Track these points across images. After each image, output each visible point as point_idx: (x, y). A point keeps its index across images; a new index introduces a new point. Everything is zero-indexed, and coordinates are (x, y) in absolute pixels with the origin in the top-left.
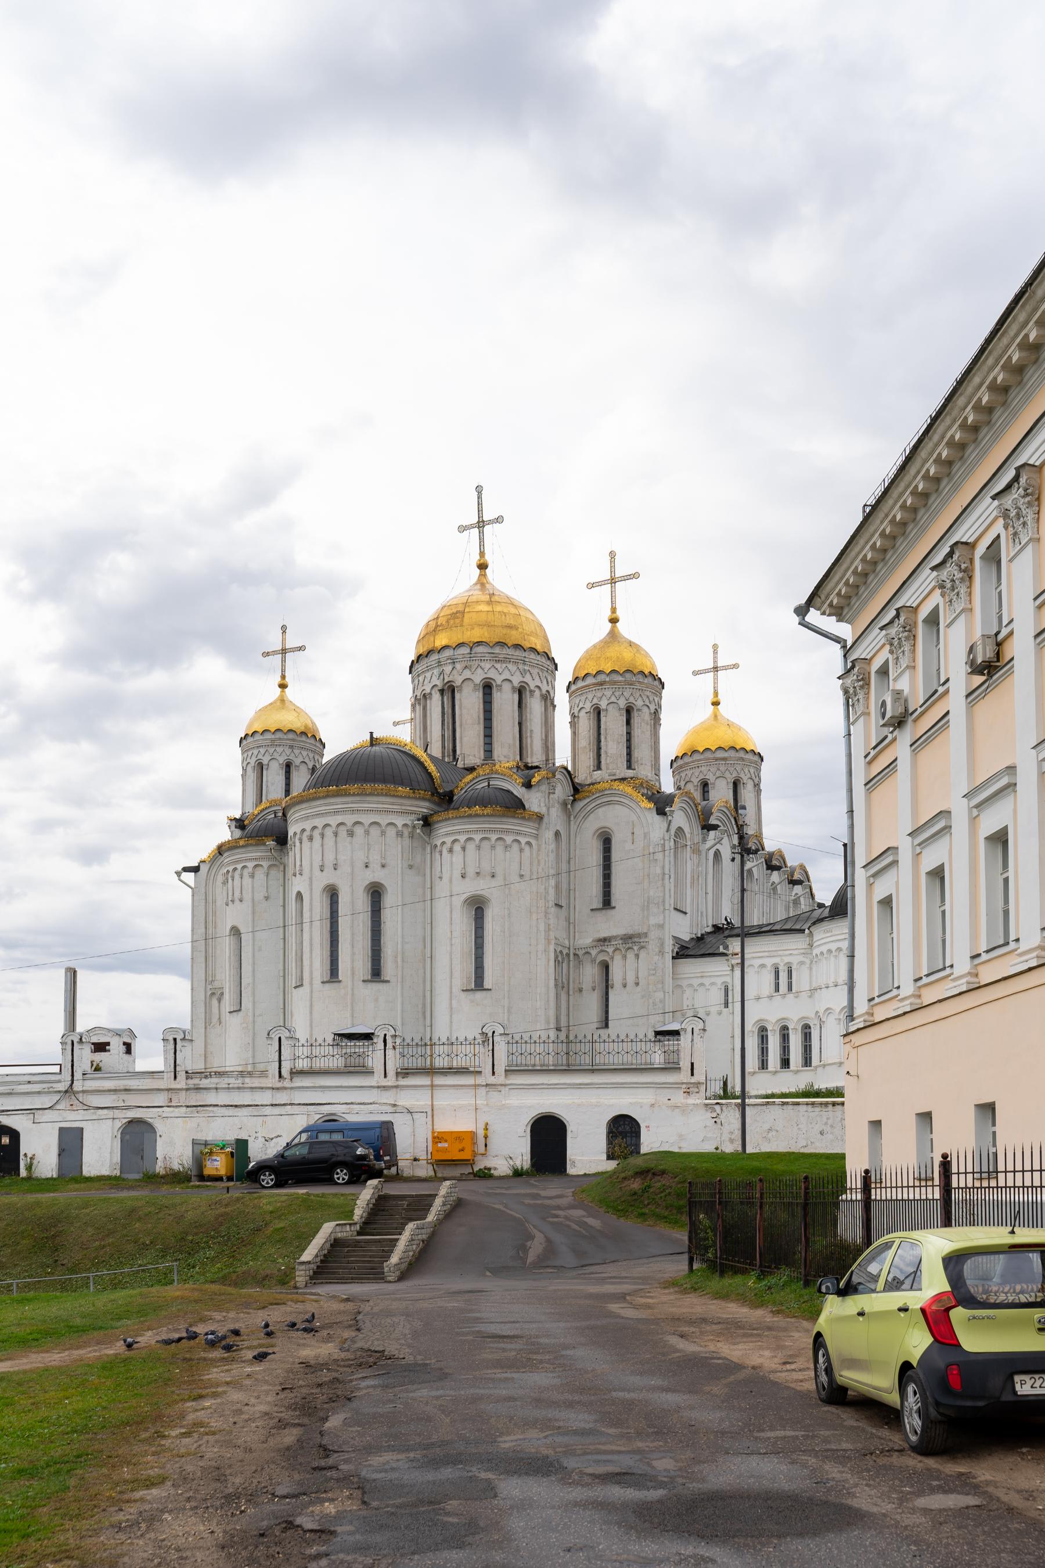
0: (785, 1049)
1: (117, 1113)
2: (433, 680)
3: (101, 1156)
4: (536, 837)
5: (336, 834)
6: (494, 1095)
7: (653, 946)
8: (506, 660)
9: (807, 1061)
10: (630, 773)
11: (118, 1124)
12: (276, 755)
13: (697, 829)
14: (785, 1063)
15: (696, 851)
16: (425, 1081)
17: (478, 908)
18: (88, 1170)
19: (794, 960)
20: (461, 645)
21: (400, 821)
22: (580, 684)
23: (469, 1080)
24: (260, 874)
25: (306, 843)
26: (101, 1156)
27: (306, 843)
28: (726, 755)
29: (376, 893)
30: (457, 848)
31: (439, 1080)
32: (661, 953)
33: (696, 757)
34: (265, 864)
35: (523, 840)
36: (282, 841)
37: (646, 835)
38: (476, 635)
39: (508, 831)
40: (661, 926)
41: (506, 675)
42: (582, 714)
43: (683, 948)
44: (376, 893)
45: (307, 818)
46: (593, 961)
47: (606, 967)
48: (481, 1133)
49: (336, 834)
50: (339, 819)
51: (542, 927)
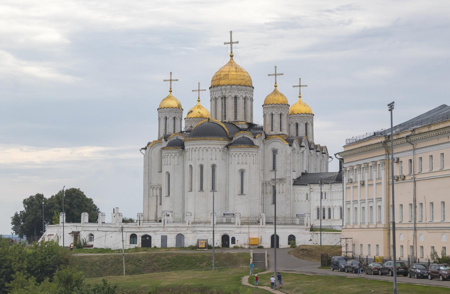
0: (324, 214)
1: (175, 232)
2: (218, 94)
3: (171, 243)
4: (257, 152)
5: (203, 150)
6: (263, 230)
7: (288, 183)
8: (241, 90)
9: (330, 217)
10: (281, 133)
11: (176, 235)
12: (171, 115)
13: (298, 146)
14: (324, 218)
15: (298, 153)
16: (247, 226)
17: (242, 172)
18: (168, 246)
19: (327, 191)
20: (228, 85)
21: (220, 147)
22: (267, 106)
23: (257, 226)
24: (176, 157)
25: (193, 152)
26: (171, 243)
27: (193, 152)
28: (304, 115)
29: (214, 167)
30: (236, 155)
31: (250, 226)
32: (290, 184)
33: (294, 115)
34: (178, 154)
35: (254, 154)
36: (183, 148)
37: (286, 151)
38: (233, 82)
39: (250, 152)
40: (290, 177)
41: (241, 94)
42: (267, 114)
43: (295, 182)
44: (214, 167)
45: (194, 145)
46: (270, 185)
47: (274, 187)
48: (260, 238)
49: (203, 150)
50: (204, 146)
51: (258, 177)
